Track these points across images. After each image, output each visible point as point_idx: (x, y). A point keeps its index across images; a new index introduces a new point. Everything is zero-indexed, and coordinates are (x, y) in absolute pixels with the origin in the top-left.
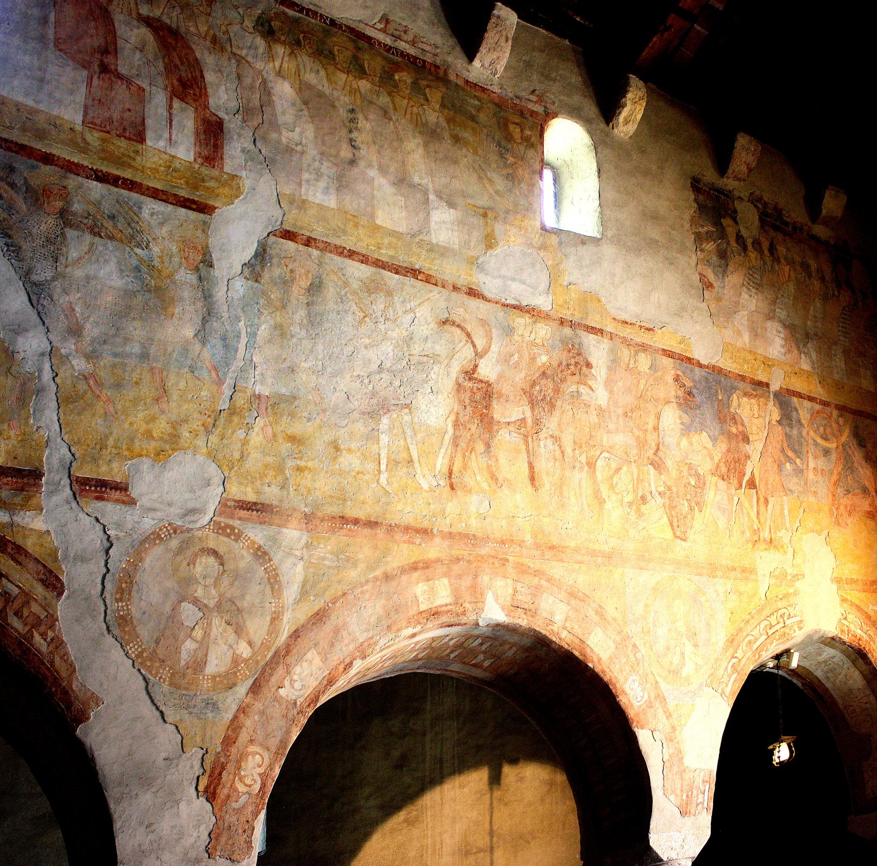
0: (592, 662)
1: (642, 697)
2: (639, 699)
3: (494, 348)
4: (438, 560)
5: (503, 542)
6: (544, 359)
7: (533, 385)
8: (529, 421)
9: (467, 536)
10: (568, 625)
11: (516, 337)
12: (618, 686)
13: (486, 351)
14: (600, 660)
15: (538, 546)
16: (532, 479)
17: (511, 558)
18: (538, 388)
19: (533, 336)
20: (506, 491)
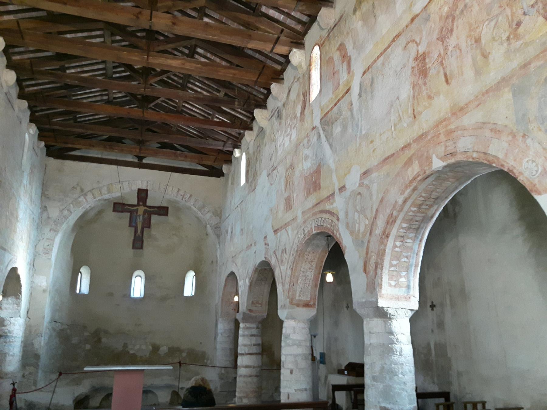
0: (494, 162)
1: (537, 171)
2: (534, 173)
3: (424, 33)
4: (413, 154)
5: (437, 126)
6: (446, 9)
7: (442, 30)
8: (442, 52)
9: (422, 135)
10: (475, 148)
11: (432, 16)
12: (515, 171)
13: (421, 39)
14: (498, 159)
15: (454, 114)
16: (447, 81)
17: (441, 131)
18: (444, 30)
19: (439, 5)
20: (436, 99)
